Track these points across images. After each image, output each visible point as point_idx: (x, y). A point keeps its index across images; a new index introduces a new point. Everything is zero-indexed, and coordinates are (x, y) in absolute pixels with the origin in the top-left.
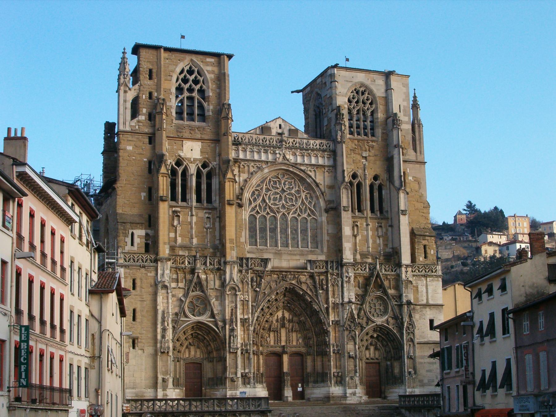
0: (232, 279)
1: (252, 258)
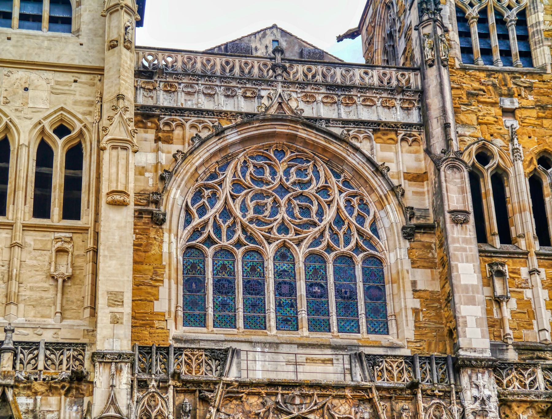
0: (112, 401)
1: (178, 351)
